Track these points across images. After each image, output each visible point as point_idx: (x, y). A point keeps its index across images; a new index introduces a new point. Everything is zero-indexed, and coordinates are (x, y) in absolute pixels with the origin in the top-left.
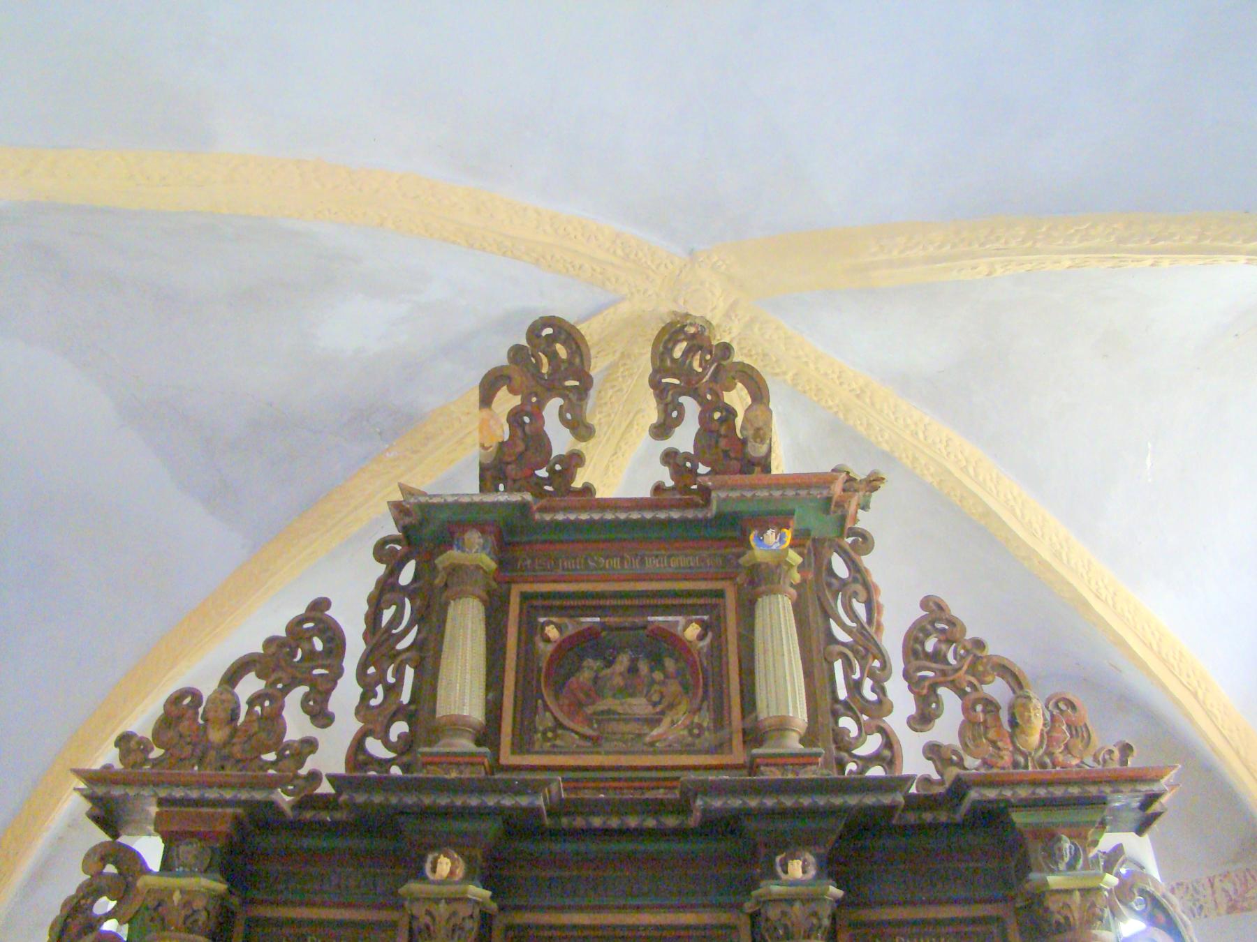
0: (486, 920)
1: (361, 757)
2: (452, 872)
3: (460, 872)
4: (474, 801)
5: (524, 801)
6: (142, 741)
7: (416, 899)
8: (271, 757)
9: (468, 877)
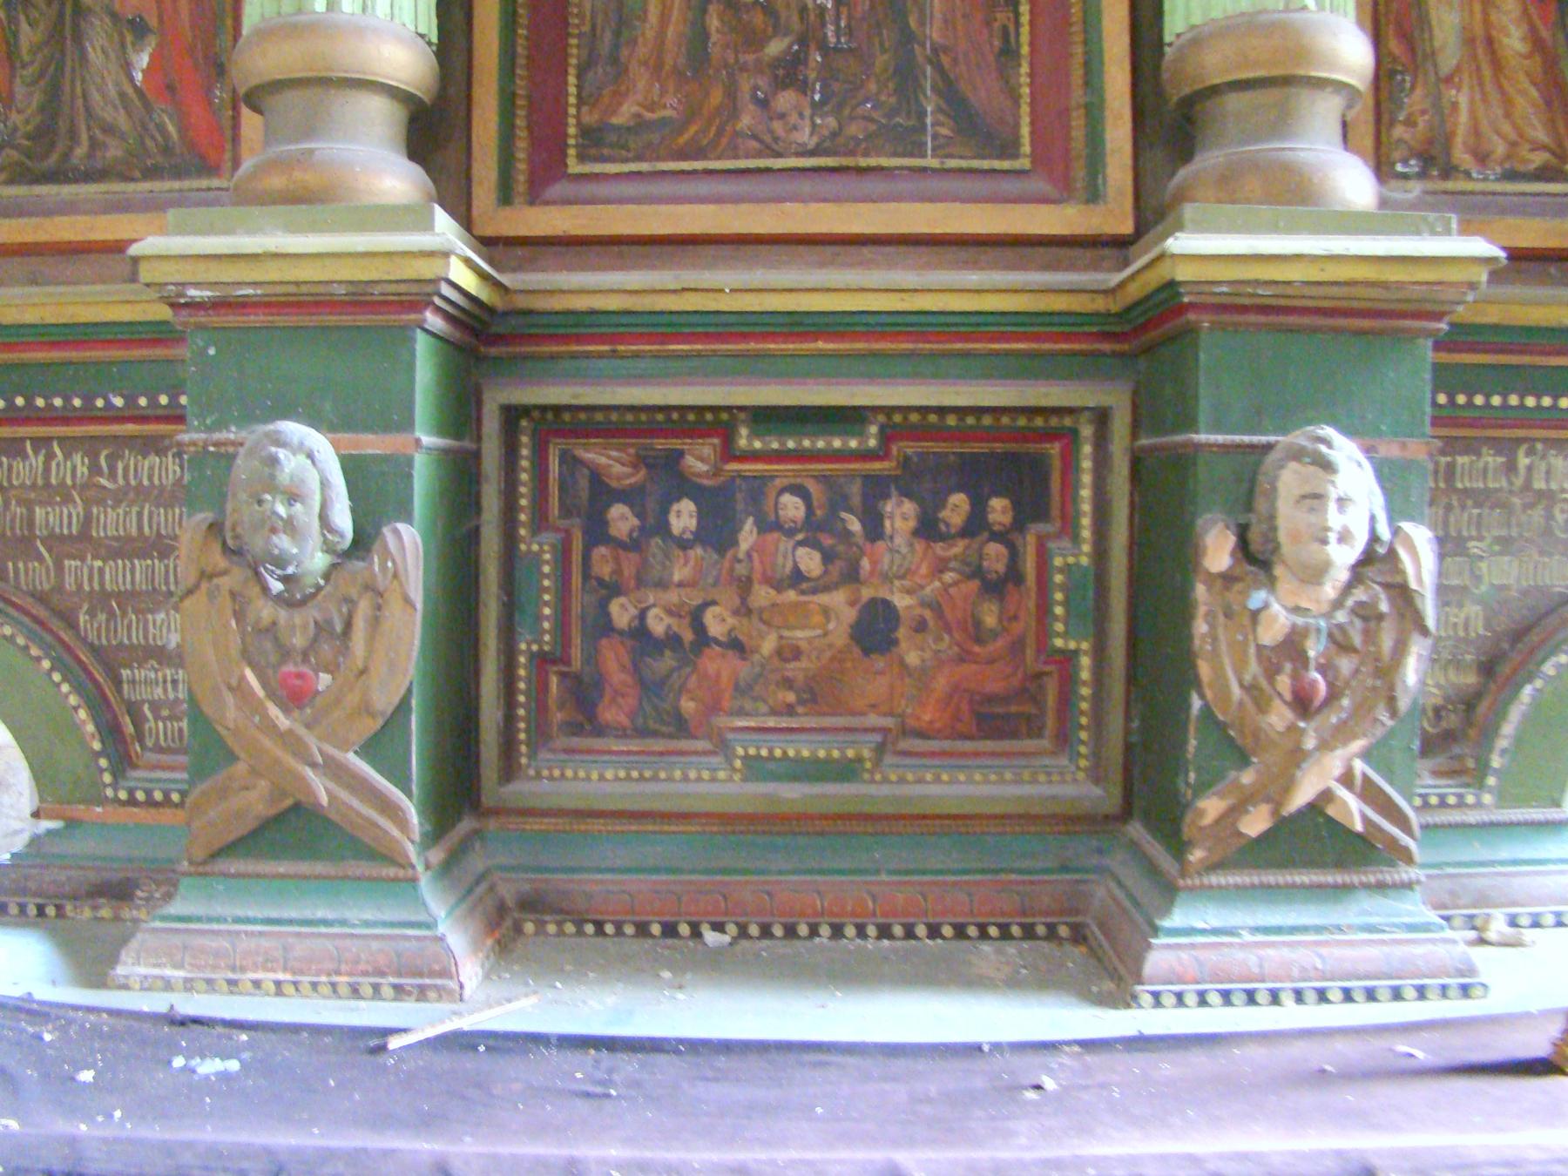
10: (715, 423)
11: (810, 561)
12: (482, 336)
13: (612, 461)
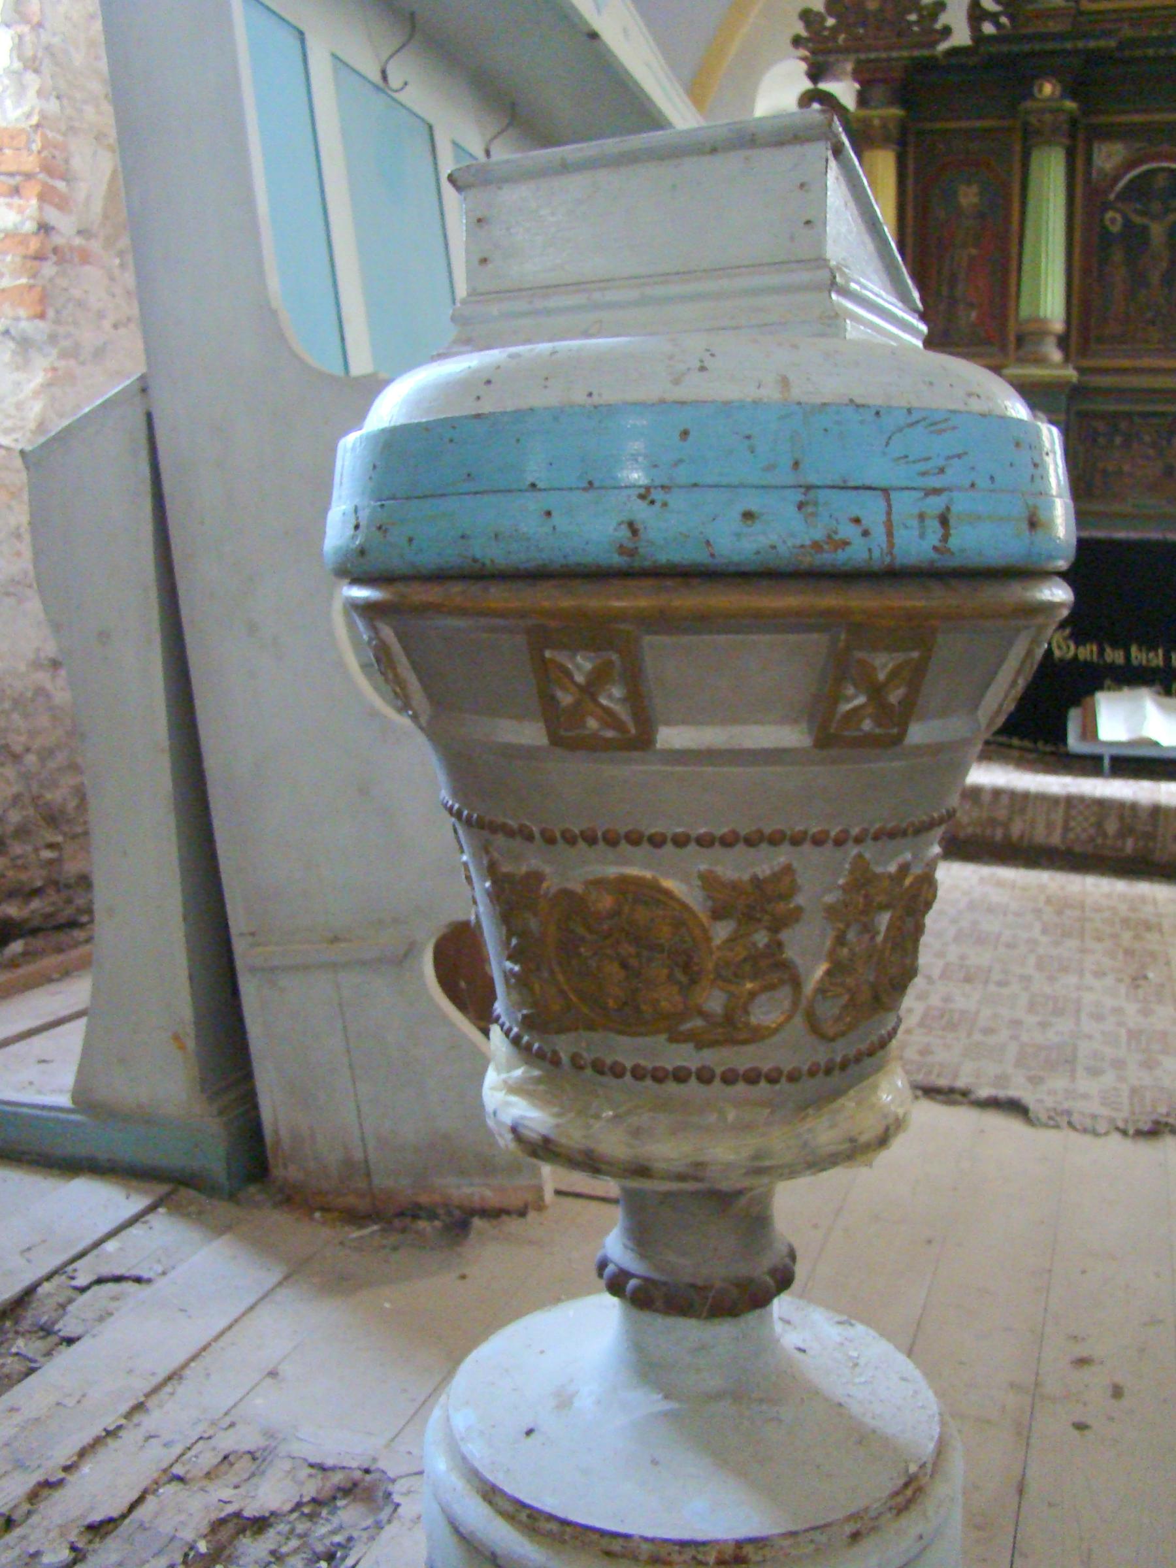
0: (1074, 122)
1: (978, 13)
2: (1053, 93)
3: (1058, 93)
4: (1068, 46)
5: (1102, 43)
6: (818, 14)
7: (1027, 112)
8: (913, 17)
9: (1063, 96)
10: (1128, 415)
11: (1151, 452)
12: (1077, 392)
13: (1100, 425)
